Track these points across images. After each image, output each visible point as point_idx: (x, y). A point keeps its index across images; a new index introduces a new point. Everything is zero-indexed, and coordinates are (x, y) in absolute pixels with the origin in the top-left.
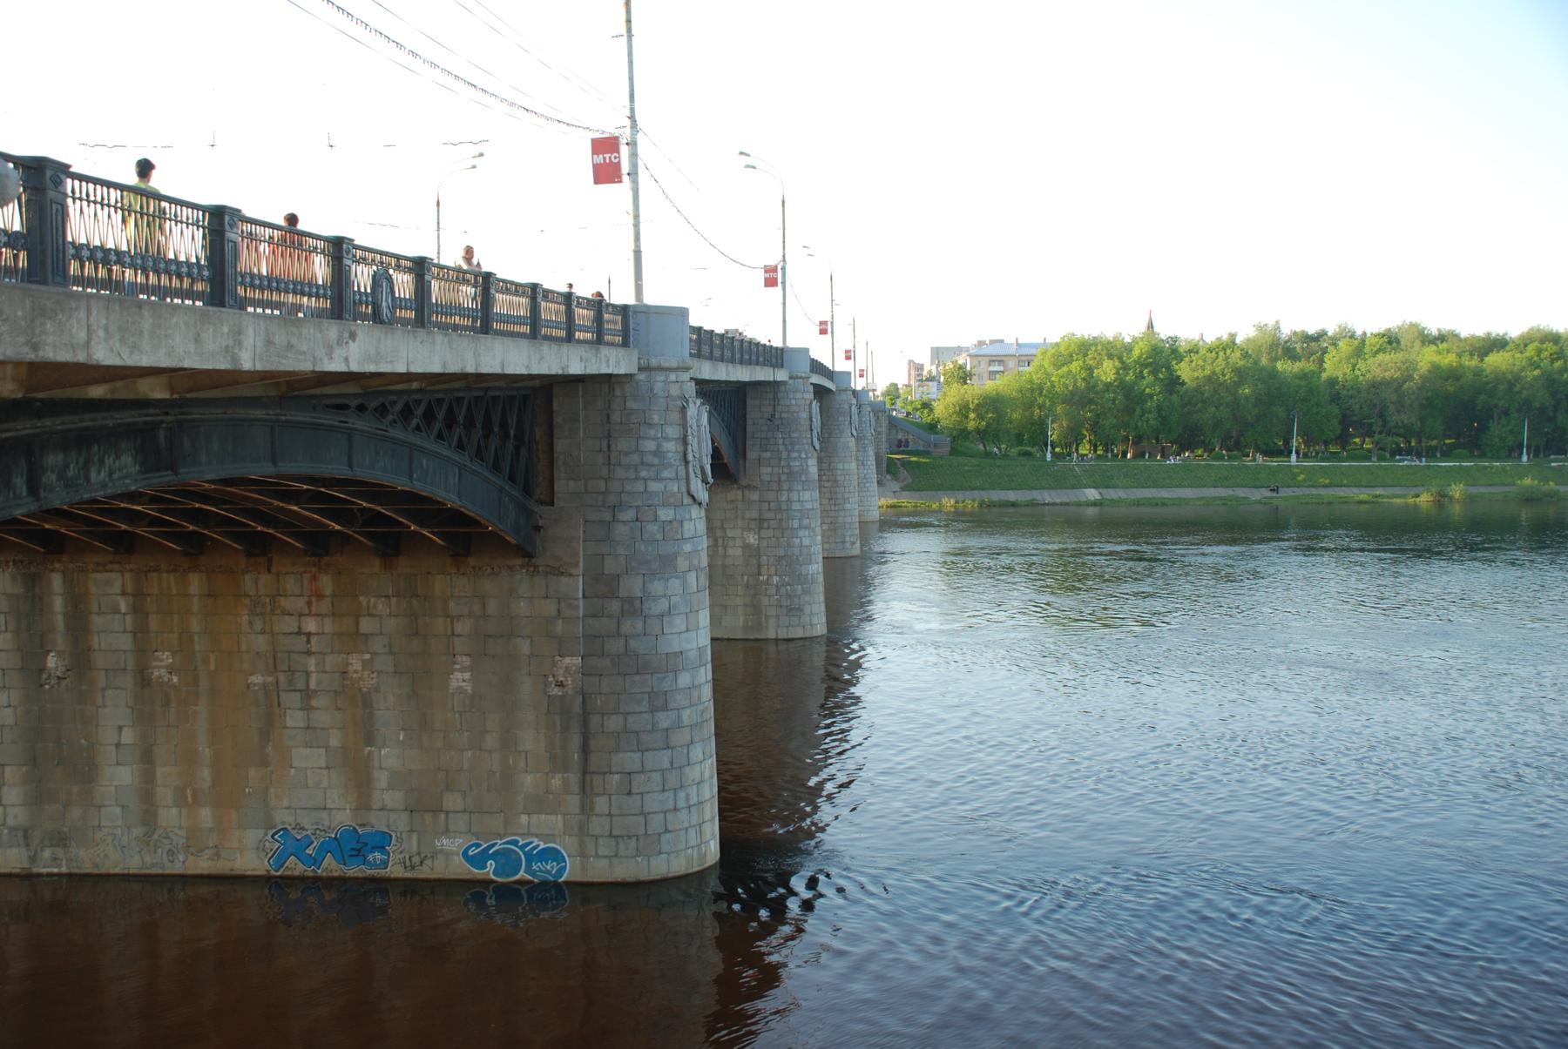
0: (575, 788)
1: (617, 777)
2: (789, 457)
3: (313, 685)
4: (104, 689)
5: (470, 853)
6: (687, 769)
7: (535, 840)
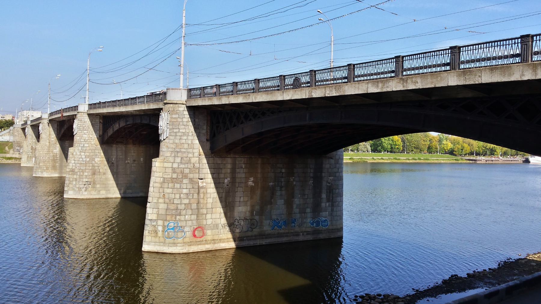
0: (331, 206)
1: (337, 203)
3: (283, 185)
4: (237, 187)
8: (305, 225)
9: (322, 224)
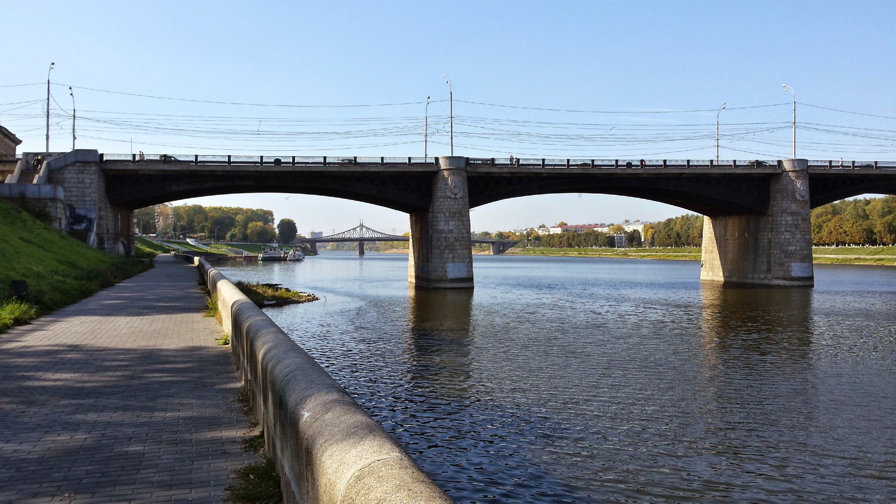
2: (782, 203)
6: (444, 255)
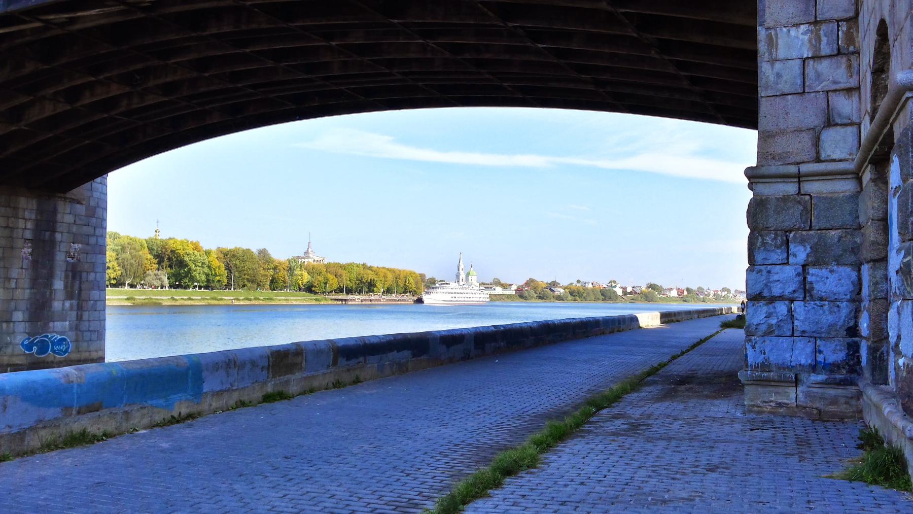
0: (75, 308)
5: (25, 343)
7: (56, 334)
8: (9, 350)
9: (53, 348)
